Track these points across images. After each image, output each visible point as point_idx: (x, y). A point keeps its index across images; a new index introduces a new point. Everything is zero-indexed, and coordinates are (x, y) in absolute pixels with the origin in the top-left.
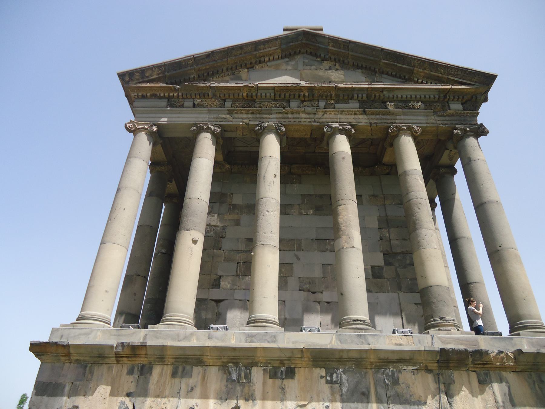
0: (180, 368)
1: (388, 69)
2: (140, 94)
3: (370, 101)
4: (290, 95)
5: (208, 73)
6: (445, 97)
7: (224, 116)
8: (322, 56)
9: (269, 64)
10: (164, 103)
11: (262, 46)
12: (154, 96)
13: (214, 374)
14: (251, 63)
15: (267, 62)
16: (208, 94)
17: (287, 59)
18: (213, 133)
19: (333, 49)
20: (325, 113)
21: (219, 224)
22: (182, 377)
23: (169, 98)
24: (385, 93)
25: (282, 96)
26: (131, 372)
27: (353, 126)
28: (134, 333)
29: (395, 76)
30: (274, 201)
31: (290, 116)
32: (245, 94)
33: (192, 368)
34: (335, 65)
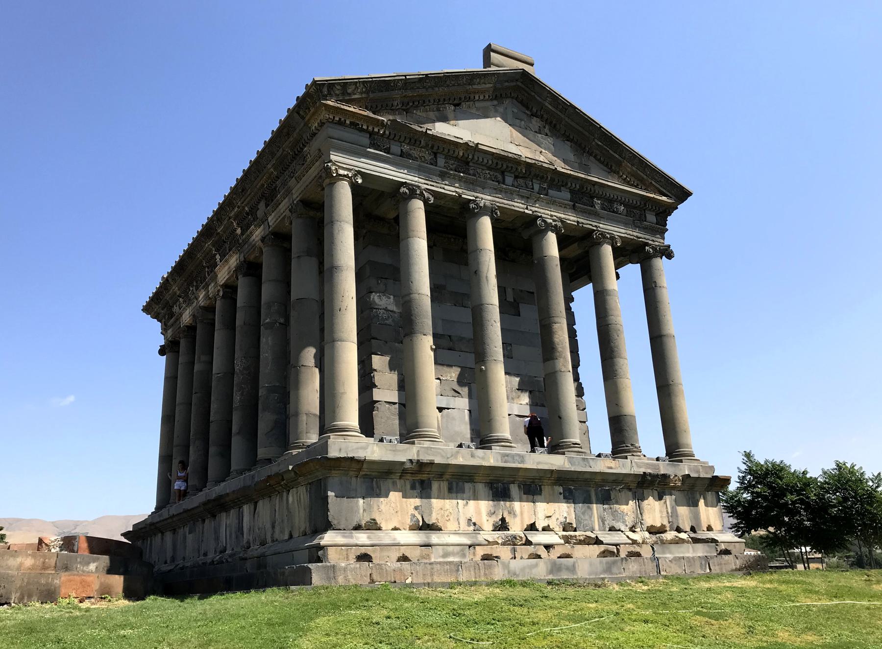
0: (454, 484)
1: (598, 152)
4: (507, 167)
8: (534, 110)
9: (478, 104)
12: (353, 125)
17: (495, 102)
18: (426, 202)
19: (550, 107)
21: (394, 309)
22: (457, 493)
23: (371, 134)
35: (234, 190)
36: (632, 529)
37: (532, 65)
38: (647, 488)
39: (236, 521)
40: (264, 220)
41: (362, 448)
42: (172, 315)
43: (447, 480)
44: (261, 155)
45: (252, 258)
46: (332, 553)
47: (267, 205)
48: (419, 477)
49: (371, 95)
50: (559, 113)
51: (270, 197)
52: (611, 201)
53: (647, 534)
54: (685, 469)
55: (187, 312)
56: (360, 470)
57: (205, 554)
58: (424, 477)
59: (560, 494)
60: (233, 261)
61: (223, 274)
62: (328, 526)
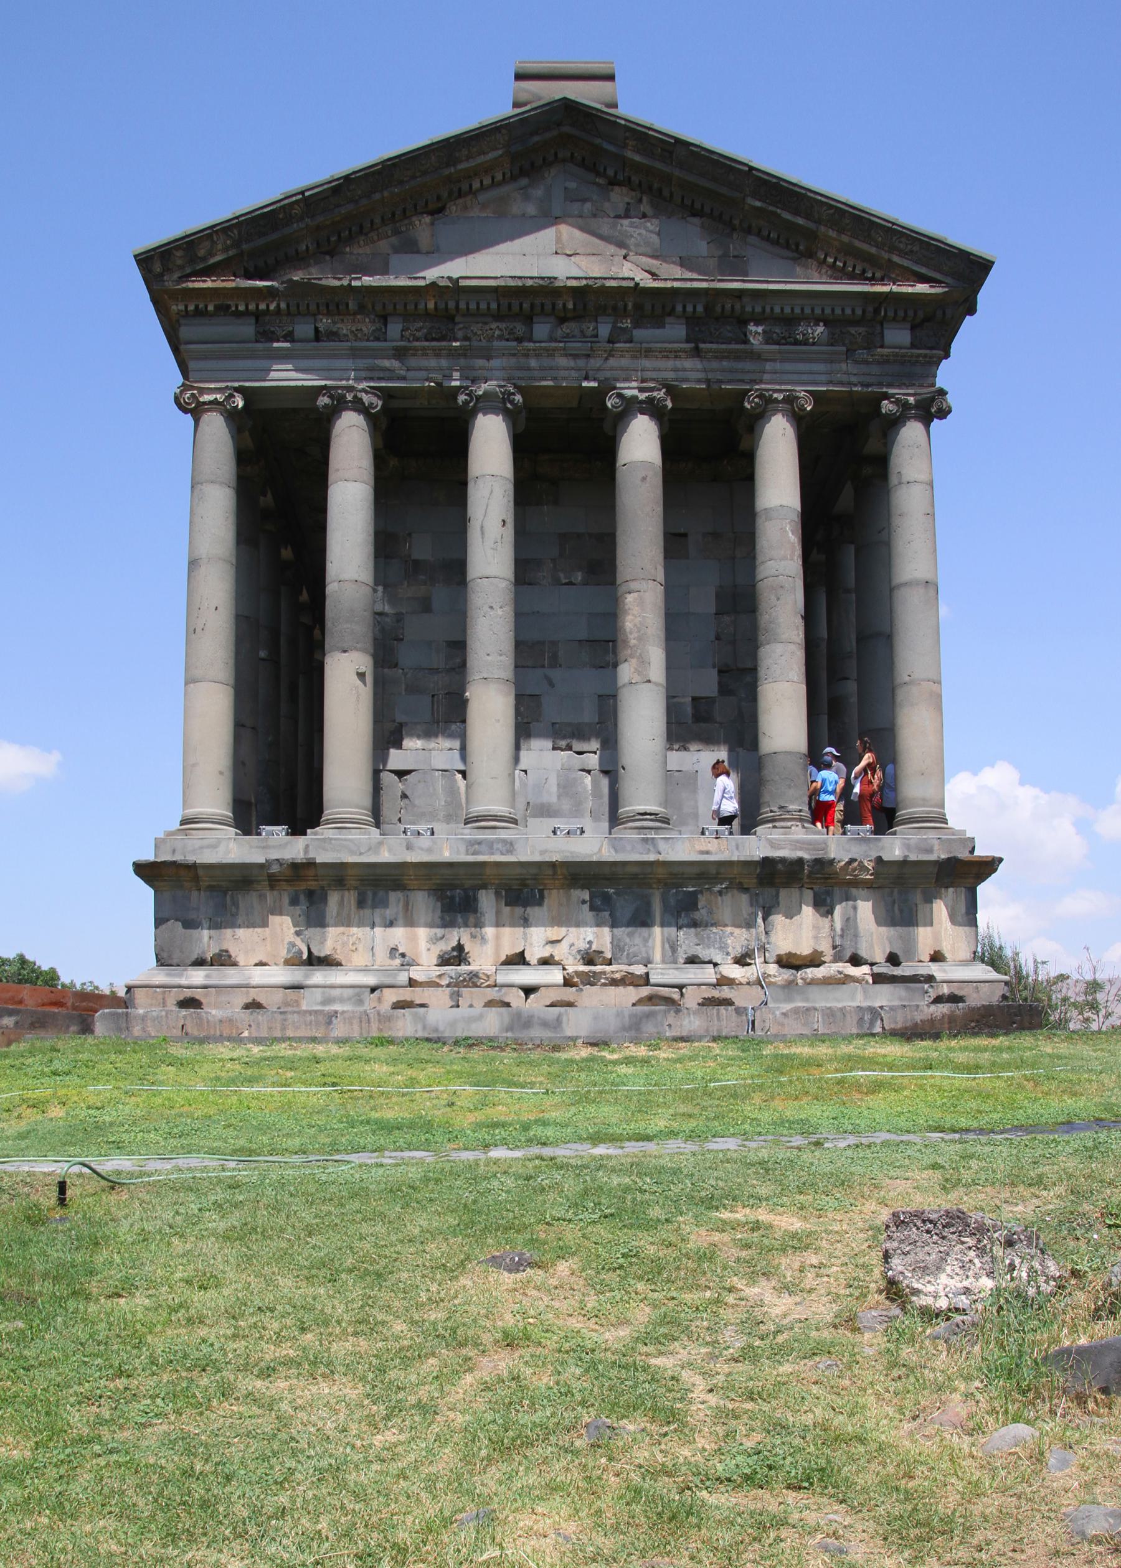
0: (370, 894)
2: (191, 308)
3: (712, 319)
4: (532, 306)
5: (339, 236)
6: (877, 311)
7: (386, 363)
8: (610, 172)
9: (483, 197)
10: (248, 329)
11: (465, 152)
13: (422, 901)
14: (439, 198)
15: (478, 191)
16: (347, 305)
17: (524, 181)
19: (637, 158)
20: (610, 354)
22: (374, 907)
23: (258, 316)
24: (745, 300)
26: (294, 902)
27: (671, 390)
28: (287, 844)
29: (776, 243)
30: (504, 584)
31: (533, 363)
32: (431, 305)
33: (387, 893)
34: (640, 201)
36: (742, 960)
37: (611, 78)
38: (787, 884)
41: (208, 847)
43: (356, 888)
48: (303, 886)
50: (658, 165)
52: (790, 321)
53: (773, 969)
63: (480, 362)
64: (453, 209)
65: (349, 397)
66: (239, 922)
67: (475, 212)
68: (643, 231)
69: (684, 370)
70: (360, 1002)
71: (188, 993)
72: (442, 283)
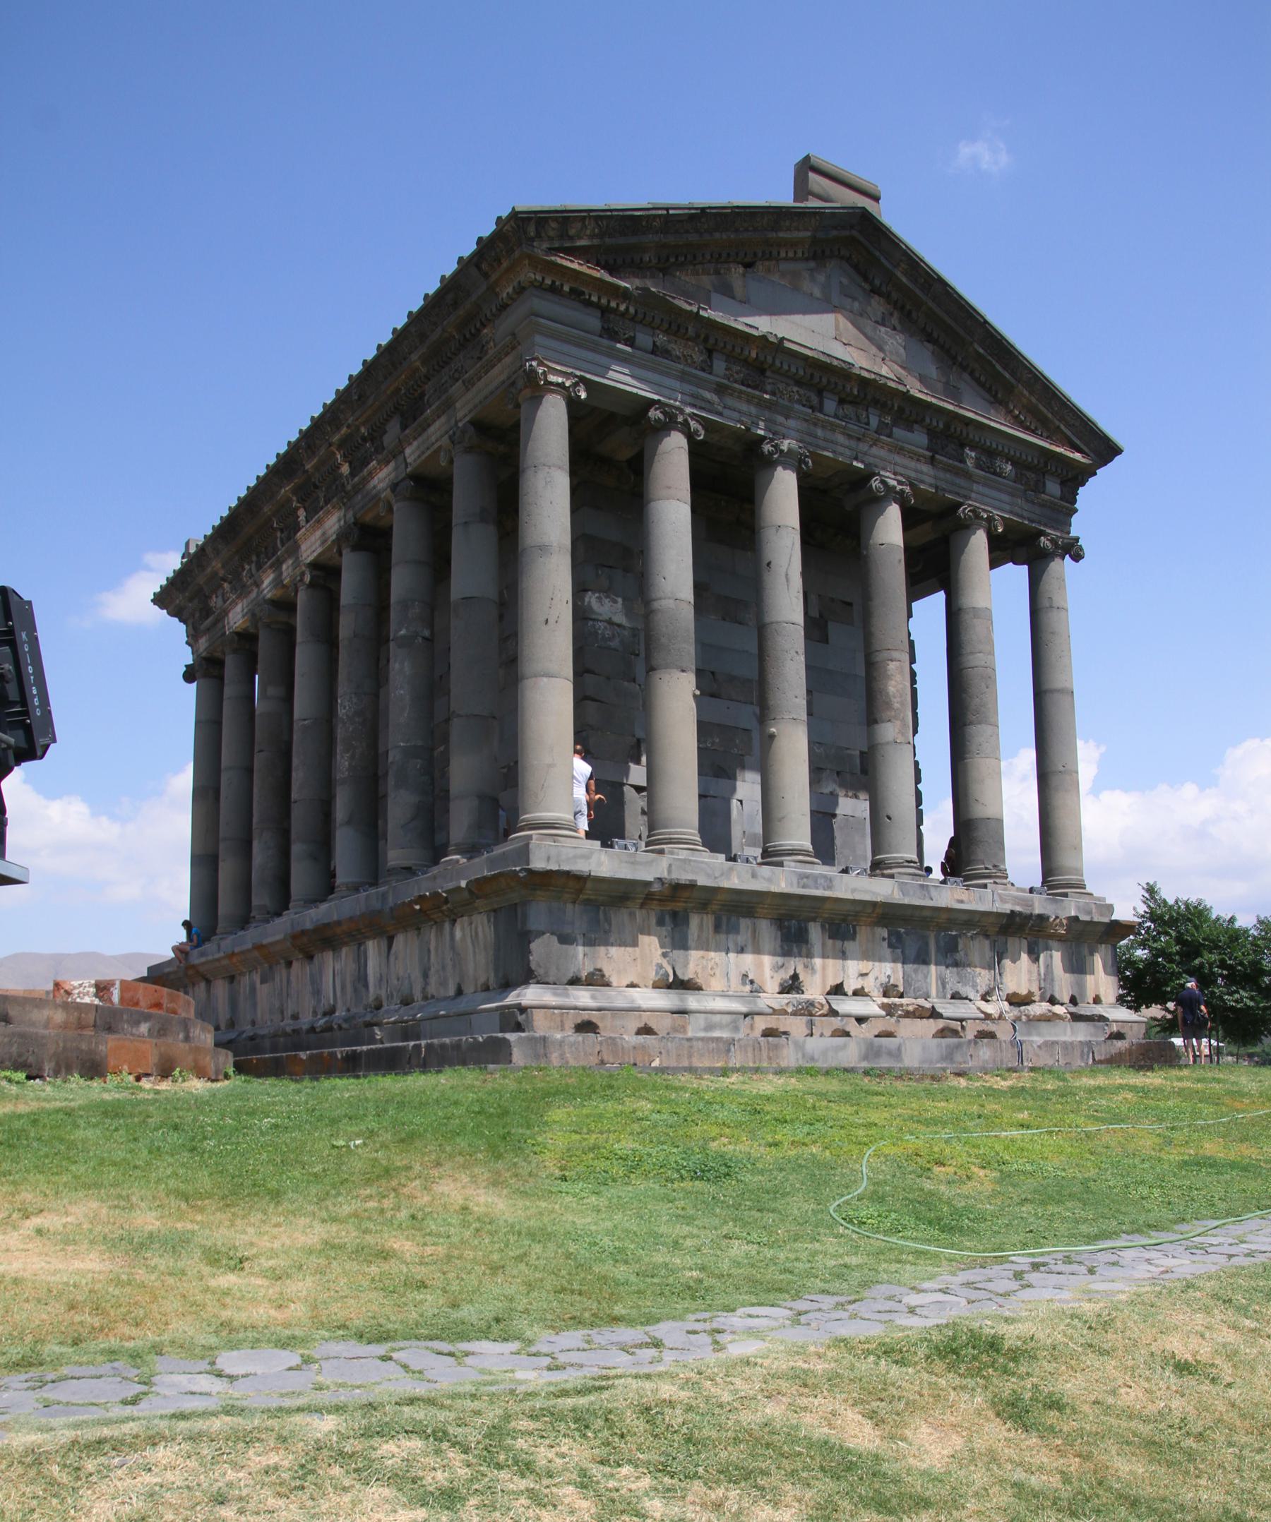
0: (724, 919)
2: (548, 282)
4: (829, 382)
7: (708, 395)
8: (877, 282)
9: (784, 266)
12: (576, 294)
13: (766, 930)
17: (812, 264)
18: (690, 436)
19: (904, 280)
23: (605, 311)
25: (816, 380)
26: (661, 922)
27: (912, 485)
29: (982, 385)
31: (820, 432)
34: (891, 314)
35: (342, 396)
39: (352, 966)
40: (397, 453)
42: (207, 612)
43: (714, 913)
44: (400, 336)
45: (368, 518)
46: (539, 1018)
47: (404, 427)
48: (670, 906)
49: (607, 240)
50: (918, 291)
51: (411, 411)
54: (1071, 908)
55: (239, 608)
56: (580, 891)
57: (295, 1017)
58: (679, 906)
59: (884, 939)
60: (333, 522)
61: (311, 545)
62: (528, 977)
63: (780, 419)
64: (760, 266)
65: (680, 419)
66: (612, 940)
67: (775, 278)
68: (895, 341)
69: (922, 473)
70: (736, 1029)
71: (585, 1016)
72: (772, 339)
